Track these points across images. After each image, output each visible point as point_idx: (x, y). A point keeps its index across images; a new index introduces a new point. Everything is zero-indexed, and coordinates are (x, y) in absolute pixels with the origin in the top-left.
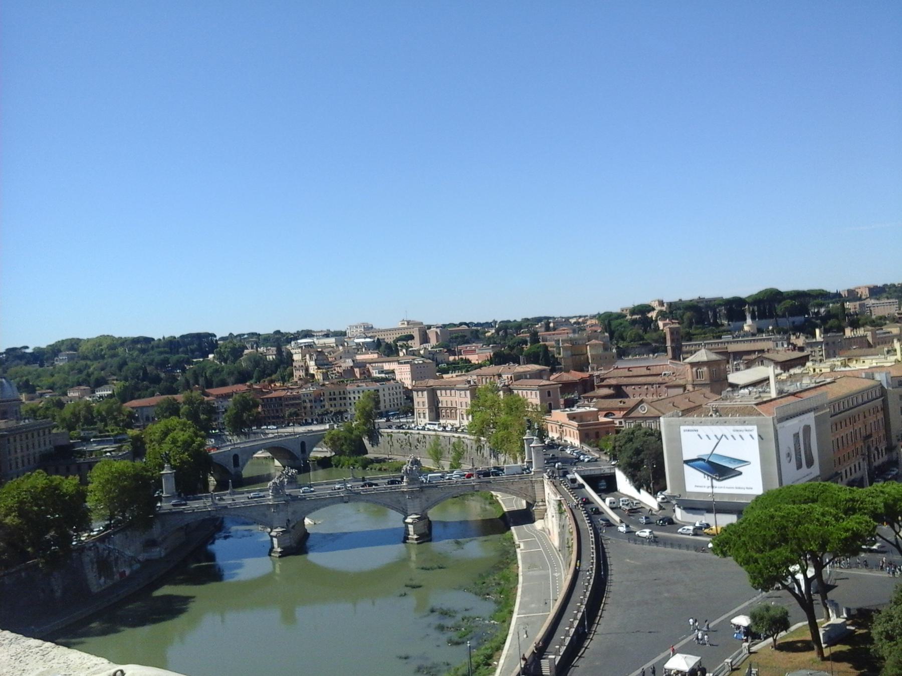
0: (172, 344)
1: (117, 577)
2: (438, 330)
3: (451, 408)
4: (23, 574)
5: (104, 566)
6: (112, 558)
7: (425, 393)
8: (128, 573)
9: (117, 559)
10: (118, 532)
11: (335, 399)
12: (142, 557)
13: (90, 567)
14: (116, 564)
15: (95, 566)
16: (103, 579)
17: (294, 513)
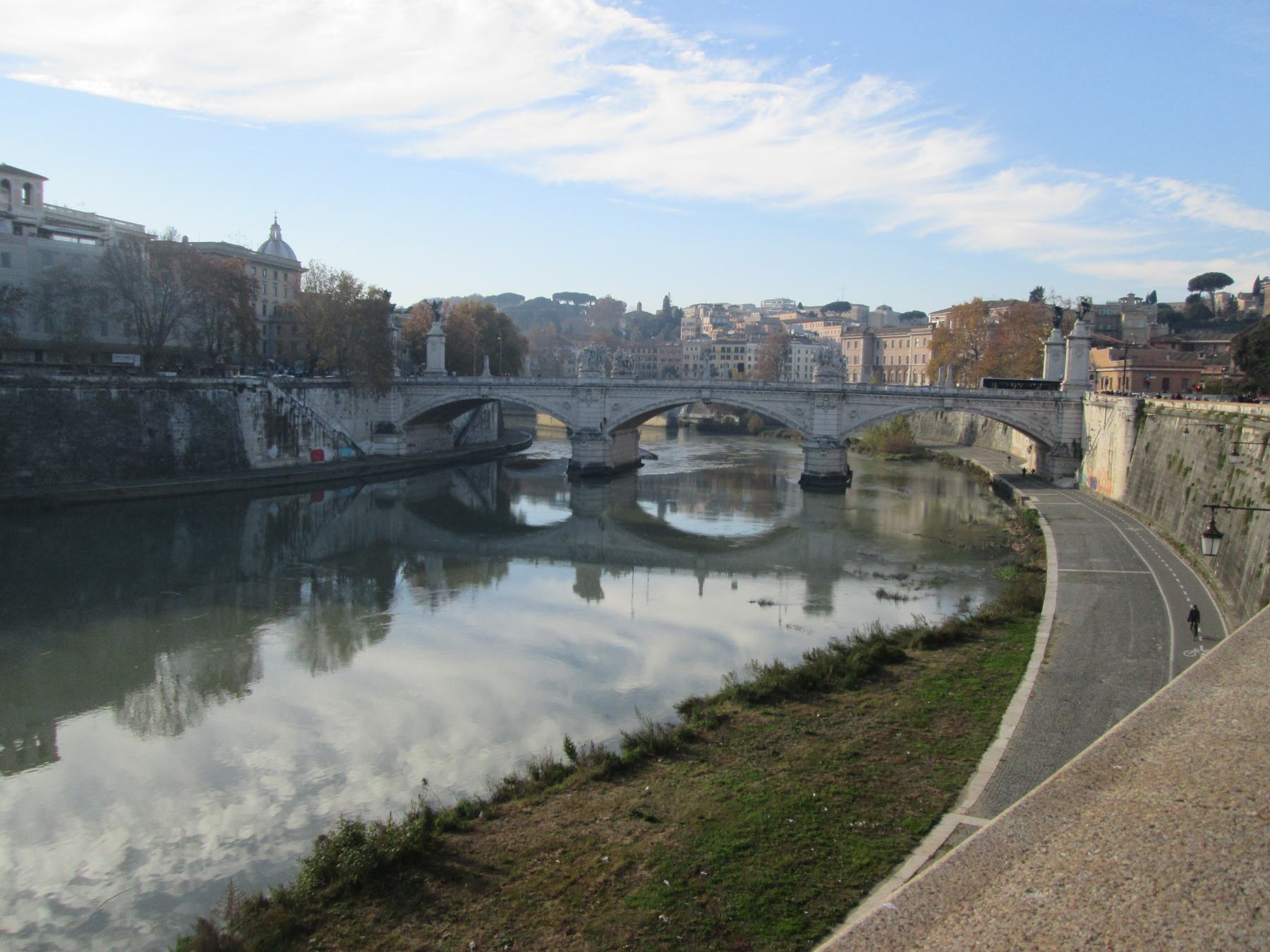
0: (541, 301)
1: (305, 456)
2: (885, 313)
3: (898, 368)
4: (114, 392)
5: (280, 428)
6: (299, 421)
7: (861, 342)
8: (329, 455)
9: (307, 425)
10: (319, 385)
11: (729, 358)
12: (368, 447)
13: (251, 419)
14: (306, 434)
15: (261, 421)
16: (274, 450)
17: (616, 408)
